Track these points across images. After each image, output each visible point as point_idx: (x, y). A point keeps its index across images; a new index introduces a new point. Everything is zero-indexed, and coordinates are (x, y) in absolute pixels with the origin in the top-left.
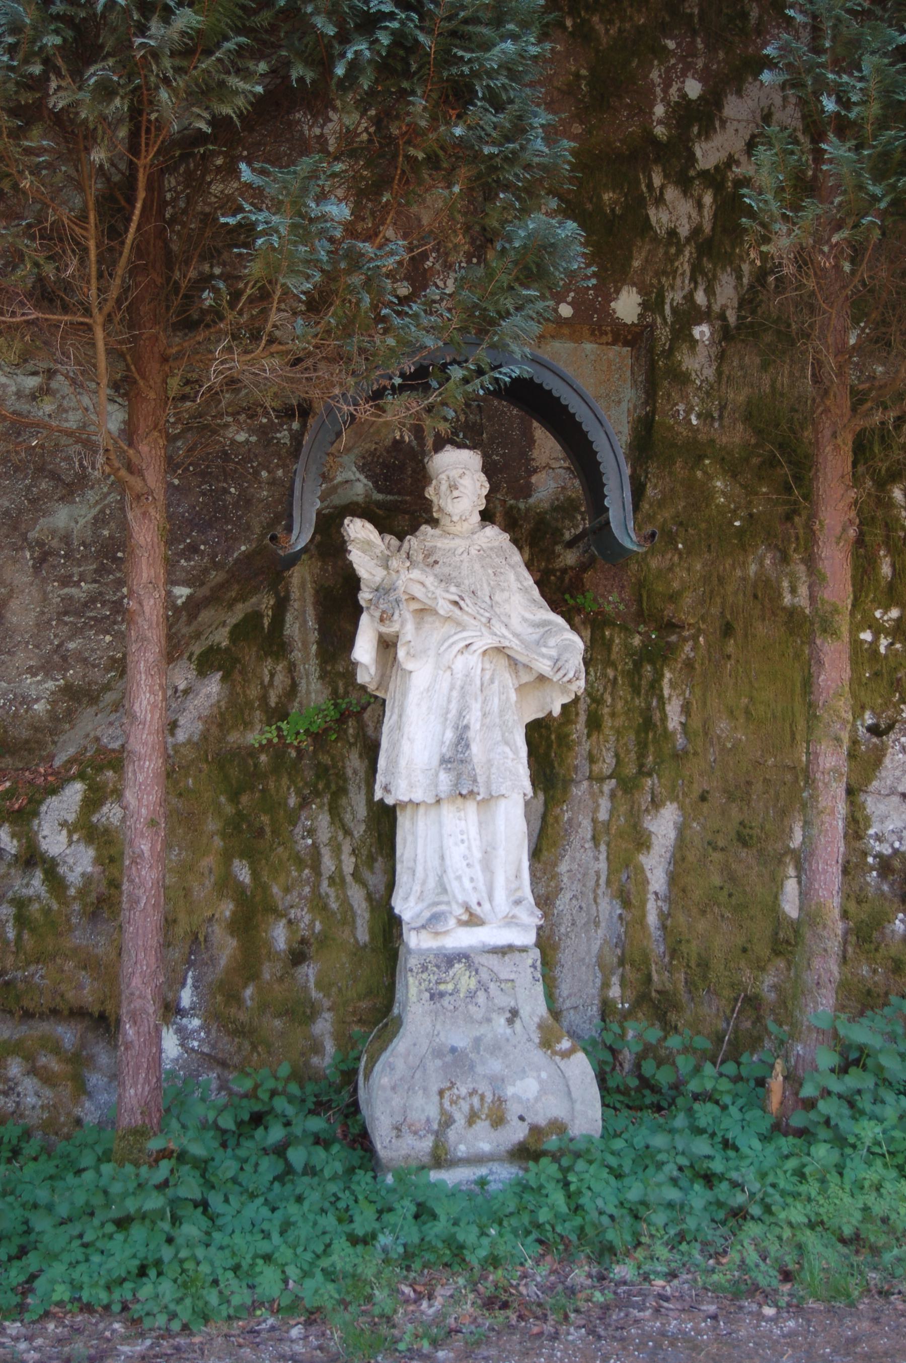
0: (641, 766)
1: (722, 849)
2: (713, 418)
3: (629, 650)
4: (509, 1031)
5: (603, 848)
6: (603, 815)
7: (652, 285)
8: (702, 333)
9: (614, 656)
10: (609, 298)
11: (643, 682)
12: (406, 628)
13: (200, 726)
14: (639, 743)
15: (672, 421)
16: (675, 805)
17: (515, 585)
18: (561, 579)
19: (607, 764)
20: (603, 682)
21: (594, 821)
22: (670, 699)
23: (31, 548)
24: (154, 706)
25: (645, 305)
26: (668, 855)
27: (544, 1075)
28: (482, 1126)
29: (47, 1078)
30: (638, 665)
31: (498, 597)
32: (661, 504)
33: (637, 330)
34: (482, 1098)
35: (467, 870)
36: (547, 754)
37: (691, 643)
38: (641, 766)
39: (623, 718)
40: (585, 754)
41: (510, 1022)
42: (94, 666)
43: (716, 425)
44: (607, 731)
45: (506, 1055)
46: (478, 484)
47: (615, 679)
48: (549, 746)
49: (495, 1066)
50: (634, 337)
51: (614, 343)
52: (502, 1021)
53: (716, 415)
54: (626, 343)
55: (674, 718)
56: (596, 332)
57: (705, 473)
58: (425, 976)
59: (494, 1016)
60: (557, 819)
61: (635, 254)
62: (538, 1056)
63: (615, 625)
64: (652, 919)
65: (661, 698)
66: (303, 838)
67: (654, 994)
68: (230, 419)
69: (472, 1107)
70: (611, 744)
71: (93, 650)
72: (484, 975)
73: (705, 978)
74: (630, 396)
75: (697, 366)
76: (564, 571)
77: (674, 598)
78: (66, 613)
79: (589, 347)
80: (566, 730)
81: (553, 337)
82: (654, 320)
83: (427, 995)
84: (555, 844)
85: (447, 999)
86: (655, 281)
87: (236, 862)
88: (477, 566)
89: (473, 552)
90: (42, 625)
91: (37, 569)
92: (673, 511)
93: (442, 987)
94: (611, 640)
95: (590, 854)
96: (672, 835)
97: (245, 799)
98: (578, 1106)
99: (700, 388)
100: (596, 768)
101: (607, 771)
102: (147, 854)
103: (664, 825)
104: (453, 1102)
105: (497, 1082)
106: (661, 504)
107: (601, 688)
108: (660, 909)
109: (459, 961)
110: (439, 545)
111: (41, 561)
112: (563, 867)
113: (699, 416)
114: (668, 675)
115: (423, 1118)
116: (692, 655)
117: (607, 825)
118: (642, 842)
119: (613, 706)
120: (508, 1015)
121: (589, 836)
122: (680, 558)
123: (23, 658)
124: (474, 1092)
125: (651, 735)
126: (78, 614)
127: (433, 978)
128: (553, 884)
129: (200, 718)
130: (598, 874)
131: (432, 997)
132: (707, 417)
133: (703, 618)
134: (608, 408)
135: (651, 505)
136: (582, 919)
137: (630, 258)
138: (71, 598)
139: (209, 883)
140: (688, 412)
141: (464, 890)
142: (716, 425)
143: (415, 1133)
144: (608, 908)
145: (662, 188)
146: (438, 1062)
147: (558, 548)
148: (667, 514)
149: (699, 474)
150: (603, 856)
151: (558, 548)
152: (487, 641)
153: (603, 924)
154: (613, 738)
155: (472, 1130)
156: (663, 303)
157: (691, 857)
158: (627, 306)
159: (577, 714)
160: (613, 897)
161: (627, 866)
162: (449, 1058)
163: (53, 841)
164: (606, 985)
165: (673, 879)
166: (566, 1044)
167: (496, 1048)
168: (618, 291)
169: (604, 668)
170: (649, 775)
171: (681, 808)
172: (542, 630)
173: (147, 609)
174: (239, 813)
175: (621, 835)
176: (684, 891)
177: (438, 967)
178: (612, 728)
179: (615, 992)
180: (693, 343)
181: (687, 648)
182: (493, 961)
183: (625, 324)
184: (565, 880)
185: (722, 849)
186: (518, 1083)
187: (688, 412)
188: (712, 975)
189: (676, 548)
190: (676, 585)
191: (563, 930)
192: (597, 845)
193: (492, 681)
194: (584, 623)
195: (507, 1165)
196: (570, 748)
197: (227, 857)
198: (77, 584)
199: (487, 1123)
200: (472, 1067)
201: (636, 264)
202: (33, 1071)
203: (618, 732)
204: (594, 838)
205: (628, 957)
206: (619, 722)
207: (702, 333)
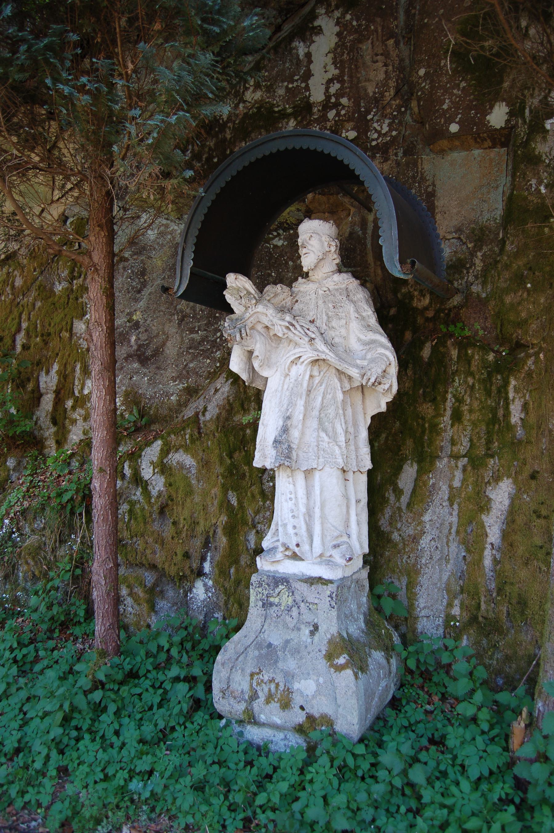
0: (488, 449)
1: (545, 517)
3: (485, 364)
4: (309, 640)
5: (456, 506)
6: (457, 483)
7: (517, 97)
9: (473, 368)
10: (485, 113)
11: (494, 388)
12: (259, 348)
13: (217, 411)
14: (488, 432)
15: (526, 193)
16: (510, 480)
17: (353, 315)
18: (448, 315)
19: (463, 446)
21: (451, 487)
22: (513, 400)
23: (178, 313)
24: (99, 398)
25: (511, 114)
26: (503, 517)
27: (321, 680)
28: (275, 706)
29: (137, 600)
30: (490, 374)
31: (334, 323)
32: (516, 255)
33: (506, 132)
34: (277, 685)
35: (292, 520)
37: (533, 358)
38: (488, 449)
39: (478, 414)
41: (312, 633)
42: (201, 376)
44: (466, 423)
45: (301, 658)
47: (473, 385)
48: (423, 432)
49: (291, 664)
50: (502, 138)
51: (494, 146)
52: (307, 632)
54: (503, 145)
56: (478, 140)
58: (260, 590)
59: (303, 627)
60: (425, 484)
61: (505, 78)
62: (322, 664)
63: (475, 345)
64: (487, 562)
66: (268, 482)
67: (480, 619)
68: (275, 234)
69: (270, 690)
70: (468, 432)
71: (201, 368)
72: (298, 598)
73: (522, 613)
74: (504, 181)
75: (547, 149)
76: (450, 310)
77: (522, 324)
78: (190, 348)
79: (476, 152)
80: (436, 420)
81: (450, 149)
83: (261, 603)
84: (422, 501)
85: (274, 608)
86: (519, 94)
87: (230, 492)
88: (320, 302)
90: (180, 355)
91: (179, 324)
92: (525, 260)
93: (272, 599)
95: (446, 510)
96: (507, 502)
97: (236, 455)
98: (340, 710)
99: (548, 165)
100: (455, 449)
101: (463, 451)
102: (98, 489)
103: (501, 495)
104: (258, 684)
105: (289, 676)
106: (516, 255)
107: (463, 391)
108: (494, 556)
109: (282, 584)
110: (302, 289)
111: (181, 320)
112: (427, 518)
113: (546, 187)
114: (513, 382)
115: (240, 689)
116: (533, 367)
117: (459, 490)
118: (483, 505)
119: (470, 405)
120: (312, 628)
121: (446, 498)
122: (529, 294)
123: (171, 372)
124: (272, 680)
125: (497, 426)
126: (196, 348)
127: (265, 592)
128: (419, 528)
130: (451, 524)
131: (264, 605)
133: (544, 339)
134: (488, 193)
135: (509, 257)
136: (437, 555)
137: (502, 82)
138: (193, 339)
139: (216, 503)
141: (287, 534)
143: (235, 698)
144: (455, 550)
145: (527, 28)
146: (257, 653)
149: (546, 230)
150: (455, 513)
152: (309, 355)
153: (451, 562)
154: (469, 428)
155: (268, 707)
156: (524, 108)
157: (520, 520)
158: (498, 116)
160: (460, 543)
161: (471, 522)
162: (264, 652)
163: (147, 472)
164: (450, 605)
165: (505, 535)
166: (341, 660)
167: (296, 652)
168: (492, 108)
169: (466, 377)
170: (492, 456)
171: (515, 482)
172: (368, 347)
173: (95, 338)
174: (232, 464)
175: (469, 499)
176: (511, 545)
177: (269, 585)
178: (469, 420)
179: (456, 611)
181: (530, 362)
182: (303, 588)
183: (496, 129)
184: (428, 526)
185: (545, 517)
186: (303, 681)
188: (528, 612)
189: (526, 287)
190: (523, 315)
191: (423, 561)
192: (451, 505)
193: (321, 383)
195: (297, 736)
196: (438, 434)
197: (225, 489)
198: (197, 332)
199: (278, 705)
200: (276, 662)
201: (506, 85)
202: (130, 594)
203: (474, 424)
204: (449, 499)
205: (466, 586)
206: (474, 416)
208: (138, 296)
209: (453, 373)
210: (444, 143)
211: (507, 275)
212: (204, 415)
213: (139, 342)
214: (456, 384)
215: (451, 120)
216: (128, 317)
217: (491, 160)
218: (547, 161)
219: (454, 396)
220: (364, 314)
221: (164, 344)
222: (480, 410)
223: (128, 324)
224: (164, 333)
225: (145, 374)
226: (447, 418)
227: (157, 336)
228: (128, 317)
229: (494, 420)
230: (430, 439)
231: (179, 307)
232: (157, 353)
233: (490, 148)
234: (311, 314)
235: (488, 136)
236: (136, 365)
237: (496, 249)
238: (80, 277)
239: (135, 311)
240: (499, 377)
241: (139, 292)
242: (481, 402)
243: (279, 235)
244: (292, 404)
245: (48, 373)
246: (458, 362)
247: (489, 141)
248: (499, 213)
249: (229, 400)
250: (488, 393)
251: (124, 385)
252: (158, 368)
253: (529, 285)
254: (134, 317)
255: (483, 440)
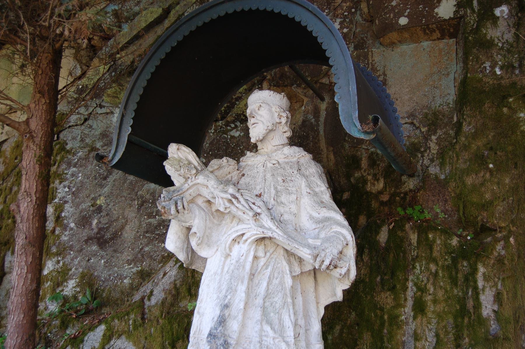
2: (514, 68)
3: (448, 250)
8: (502, 12)
9: (435, 254)
11: (460, 275)
12: (197, 223)
13: (163, 295)
14: (457, 326)
15: (481, 76)
17: (305, 189)
18: (404, 199)
20: (427, 274)
22: (483, 290)
24: (20, 276)
30: (455, 261)
31: (283, 198)
32: (475, 136)
36: (380, 331)
37: (502, 243)
39: (443, 304)
40: (411, 332)
42: (155, 260)
43: (517, 72)
44: (430, 315)
46: (276, 115)
48: (382, 324)
51: (442, 38)
53: (516, 65)
54: (451, 36)
55: (488, 306)
57: (510, 108)
63: (435, 229)
65: (475, 288)
68: (233, 126)
70: (433, 326)
71: (155, 252)
74: (455, 69)
75: (499, 34)
76: (406, 194)
77: (485, 206)
78: (147, 232)
79: (425, 44)
80: (396, 312)
81: (400, 42)
82: (466, 13)
88: (269, 176)
89: (269, 165)
90: (137, 238)
92: (485, 140)
94: (434, 241)
99: (502, 48)
106: (475, 136)
107: (425, 279)
110: (250, 163)
113: (501, 68)
114: (481, 270)
116: (503, 252)
119: (434, 294)
122: (491, 175)
123: (127, 255)
125: (466, 320)
126: (152, 232)
129: (164, 290)
132: (508, 67)
133: (513, 222)
134: (440, 79)
135: (466, 138)
138: (150, 224)
140: (493, 67)
142: (517, 72)
147: (404, 178)
148: (480, 143)
151: (404, 178)
152: (253, 231)
154: (434, 321)
159: (406, 300)
169: (428, 264)
172: (321, 225)
173: (22, 210)
178: (433, 312)
180: (495, 20)
181: (499, 247)
187: (493, 67)
189: (488, 167)
190: (488, 196)
193: (266, 266)
194: (412, 228)
196: (399, 327)
198: (155, 217)
203: (440, 316)
206: (440, 307)
207: (502, 12)
208: (104, 182)
209: (413, 260)
210: (394, 36)
211: (466, 155)
212: (149, 300)
213: (100, 226)
214: (417, 271)
215: (400, 14)
216: (93, 202)
217: (440, 51)
218: (500, 45)
219: (416, 284)
220: (317, 190)
221: (123, 228)
222: (446, 301)
223: (92, 208)
224: (123, 217)
225: (102, 257)
226: (408, 309)
227: (117, 220)
228: (93, 202)
229: (463, 312)
230: (390, 333)
231: (140, 193)
232: (116, 236)
233: (438, 39)
234: (258, 188)
235: (437, 27)
236: (95, 248)
237: (451, 132)
238: (54, 165)
239: (100, 195)
240: (465, 264)
241: (105, 178)
242: (446, 291)
243: (236, 127)
244: (231, 290)
245: (13, 253)
246: (418, 247)
247: (437, 32)
248: (451, 98)
249: (175, 285)
250: (454, 282)
251: (81, 266)
252: (115, 251)
253: (491, 166)
254: (98, 202)
255: (451, 335)
